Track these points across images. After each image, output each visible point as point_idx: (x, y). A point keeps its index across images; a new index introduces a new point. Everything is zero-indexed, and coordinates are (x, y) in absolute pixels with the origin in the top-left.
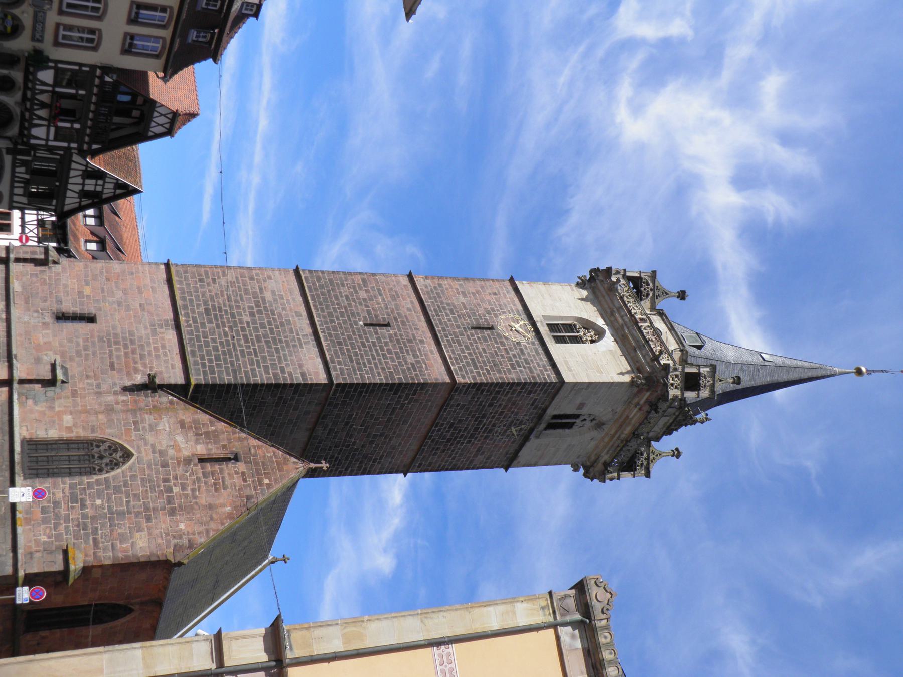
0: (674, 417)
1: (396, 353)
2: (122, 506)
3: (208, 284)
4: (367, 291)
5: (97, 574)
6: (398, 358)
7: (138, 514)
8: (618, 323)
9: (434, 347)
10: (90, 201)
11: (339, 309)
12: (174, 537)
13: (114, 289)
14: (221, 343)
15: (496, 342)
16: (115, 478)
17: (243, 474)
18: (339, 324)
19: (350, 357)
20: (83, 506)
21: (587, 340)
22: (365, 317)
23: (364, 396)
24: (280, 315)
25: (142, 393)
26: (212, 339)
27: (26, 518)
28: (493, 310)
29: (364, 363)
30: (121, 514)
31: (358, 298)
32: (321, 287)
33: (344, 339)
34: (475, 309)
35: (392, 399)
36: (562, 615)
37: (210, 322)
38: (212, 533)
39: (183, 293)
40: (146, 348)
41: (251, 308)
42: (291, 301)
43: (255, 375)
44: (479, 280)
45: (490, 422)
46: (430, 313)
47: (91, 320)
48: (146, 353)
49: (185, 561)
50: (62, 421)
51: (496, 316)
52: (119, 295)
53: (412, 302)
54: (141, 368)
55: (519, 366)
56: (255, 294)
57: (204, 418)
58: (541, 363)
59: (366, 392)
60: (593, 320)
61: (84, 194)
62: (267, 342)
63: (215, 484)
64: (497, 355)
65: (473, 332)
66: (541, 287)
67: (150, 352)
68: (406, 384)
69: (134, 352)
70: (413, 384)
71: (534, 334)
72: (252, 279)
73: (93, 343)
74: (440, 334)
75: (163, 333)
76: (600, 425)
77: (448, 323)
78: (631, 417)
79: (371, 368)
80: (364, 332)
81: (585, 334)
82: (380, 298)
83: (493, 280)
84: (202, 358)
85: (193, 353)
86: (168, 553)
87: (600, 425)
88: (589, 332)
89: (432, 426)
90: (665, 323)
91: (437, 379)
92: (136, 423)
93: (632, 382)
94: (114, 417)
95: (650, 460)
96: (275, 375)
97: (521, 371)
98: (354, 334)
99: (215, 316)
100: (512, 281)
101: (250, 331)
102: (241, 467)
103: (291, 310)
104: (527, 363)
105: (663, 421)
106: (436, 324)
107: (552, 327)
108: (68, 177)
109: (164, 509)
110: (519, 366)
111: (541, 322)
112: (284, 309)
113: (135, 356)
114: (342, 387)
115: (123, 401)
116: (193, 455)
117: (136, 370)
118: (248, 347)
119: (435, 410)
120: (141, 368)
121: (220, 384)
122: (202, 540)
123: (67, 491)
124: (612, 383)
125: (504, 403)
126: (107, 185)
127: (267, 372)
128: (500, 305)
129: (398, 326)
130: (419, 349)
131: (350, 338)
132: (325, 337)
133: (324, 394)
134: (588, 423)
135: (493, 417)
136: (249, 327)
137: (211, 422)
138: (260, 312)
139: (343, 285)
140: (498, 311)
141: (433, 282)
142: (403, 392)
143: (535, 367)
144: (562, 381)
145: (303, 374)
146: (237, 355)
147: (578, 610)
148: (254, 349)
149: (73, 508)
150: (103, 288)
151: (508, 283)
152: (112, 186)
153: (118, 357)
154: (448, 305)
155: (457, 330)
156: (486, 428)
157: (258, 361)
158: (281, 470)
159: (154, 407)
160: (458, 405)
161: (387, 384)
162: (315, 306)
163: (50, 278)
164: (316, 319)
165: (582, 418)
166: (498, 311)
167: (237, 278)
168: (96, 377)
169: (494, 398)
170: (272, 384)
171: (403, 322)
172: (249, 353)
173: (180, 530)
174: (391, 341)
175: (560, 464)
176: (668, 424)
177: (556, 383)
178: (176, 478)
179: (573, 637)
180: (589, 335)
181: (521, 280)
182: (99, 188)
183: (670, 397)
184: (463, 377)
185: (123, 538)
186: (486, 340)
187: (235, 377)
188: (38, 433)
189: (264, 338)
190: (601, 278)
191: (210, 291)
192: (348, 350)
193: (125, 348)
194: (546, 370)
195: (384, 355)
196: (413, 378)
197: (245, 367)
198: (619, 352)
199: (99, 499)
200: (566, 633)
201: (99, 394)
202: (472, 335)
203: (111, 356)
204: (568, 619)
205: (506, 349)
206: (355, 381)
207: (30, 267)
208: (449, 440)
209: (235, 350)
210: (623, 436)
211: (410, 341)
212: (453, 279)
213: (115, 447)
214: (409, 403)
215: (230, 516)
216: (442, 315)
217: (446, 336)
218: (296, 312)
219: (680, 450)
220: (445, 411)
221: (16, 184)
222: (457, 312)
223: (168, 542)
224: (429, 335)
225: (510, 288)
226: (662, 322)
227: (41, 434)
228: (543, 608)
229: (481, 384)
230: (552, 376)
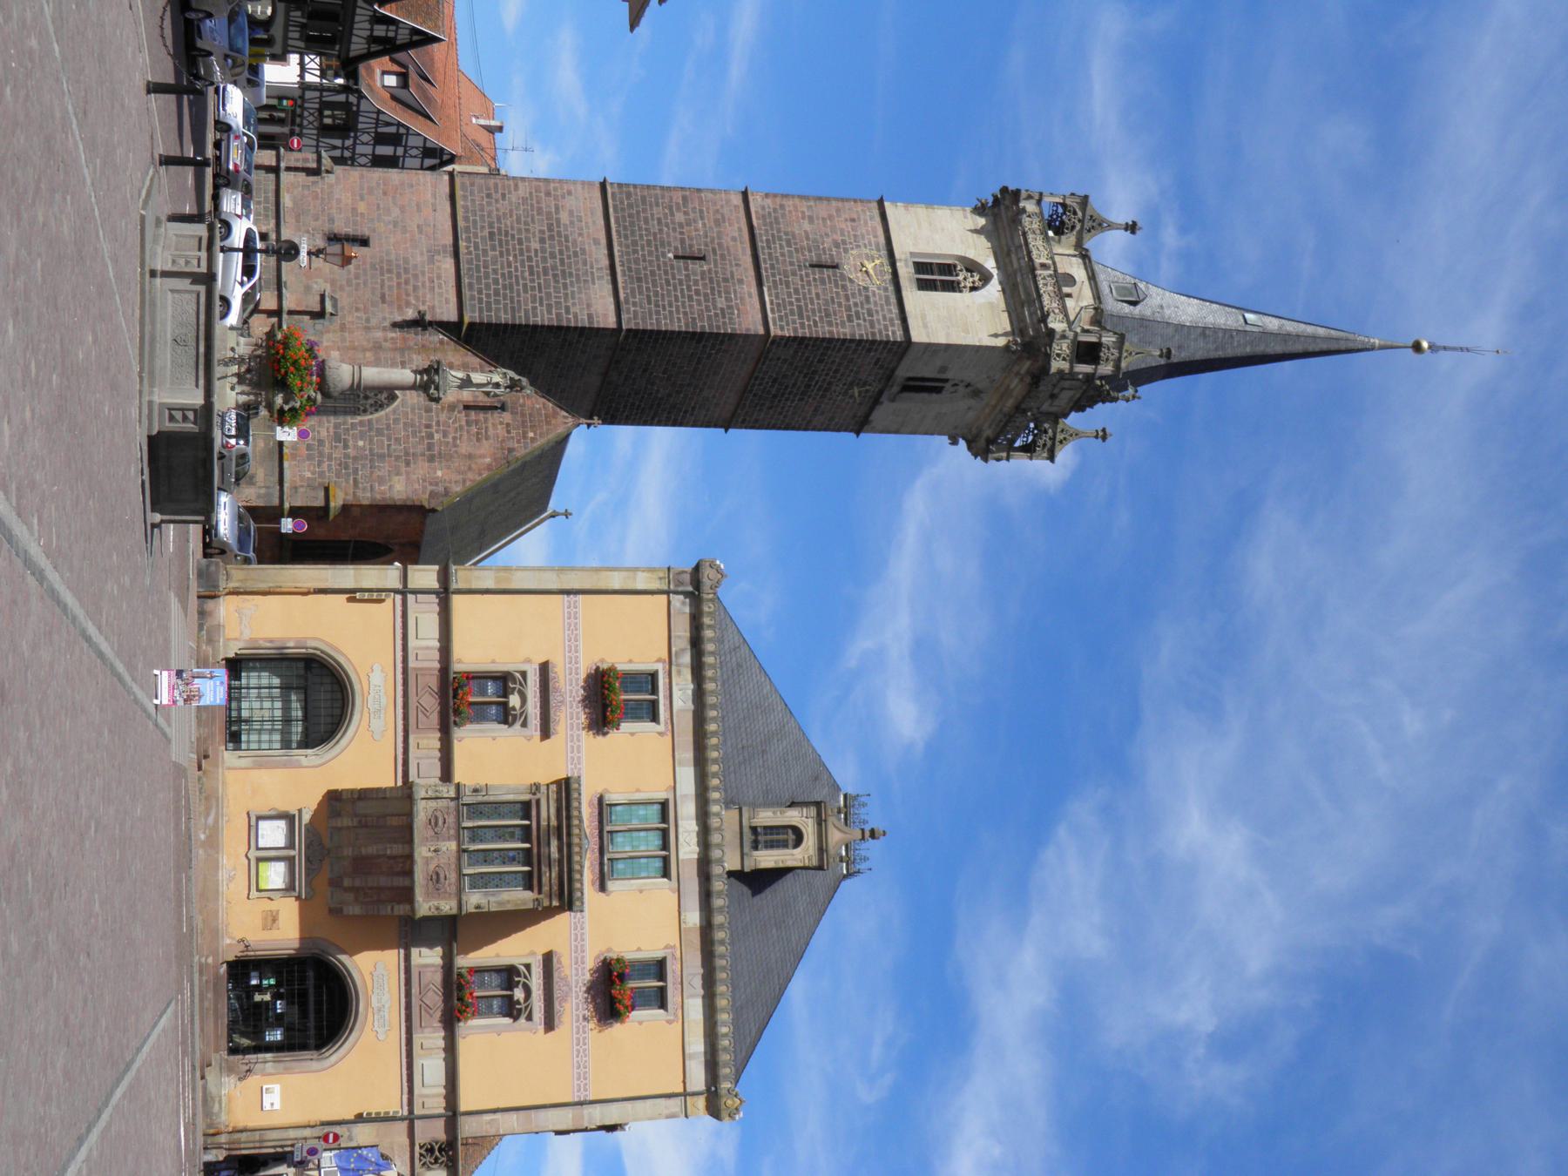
1: (706, 295)
2: (383, 448)
3: (497, 201)
4: (686, 213)
5: (356, 512)
7: (398, 458)
8: (1012, 266)
9: (754, 290)
10: (381, 48)
11: (646, 235)
12: (431, 484)
14: (503, 275)
15: (837, 286)
16: (378, 420)
17: (508, 425)
18: (643, 255)
19: (648, 297)
20: (346, 446)
21: (965, 287)
22: (676, 248)
24: (575, 241)
25: (412, 330)
26: (493, 270)
27: (292, 454)
28: (844, 242)
29: (664, 306)
30: (381, 457)
31: (673, 223)
33: (646, 275)
34: (820, 240)
36: (676, 586)
37: (493, 249)
38: (468, 484)
39: (467, 211)
40: (421, 278)
41: (542, 232)
42: (590, 224)
43: (535, 315)
44: (837, 199)
45: (824, 380)
48: (420, 284)
49: (439, 508)
51: (846, 251)
52: (396, 212)
53: (740, 229)
54: (413, 302)
55: (858, 318)
56: (549, 213)
58: (888, 316)
59: (663, 339)
60: (980, 260)
61: (372, 39)
62: (555, 276)
63: (478, 433)
64: (833, 302)
66: (921, 211)
68: (711, 334)
69: (407, 282)
71: (890, 277)
72: (548, 194)
75: (439, 261)
76: (977, 393)
77: (780, 258)
78: (1012, 386)
79: (671, 312)
80: (672, 268)
81: (965, 279)
83: (855, 201)
84: (480, 292)
85: (471, 285)
86: (424, 499)
87: (977, 393)
88: (972, 276)
89: (750, 379)
90: (1086, 269)
91: (748, 329)
93: (1007, 348)
94: (382, 355)
95: (1057, 440)
97: (859, 325)
98: (659, 269)
99: (500, 241)
100: (881, 203)
101: (537, 261)
102: (507, 417)
103: (589, 236)
104: (870, 313)
106: (765, 259)
107: (921, 267)
108: (353, 22)
109: (423, 455)
110: (858, 318)
111: (906, 260)
112: (580, 235)
113: (408, 287)
114: (634, 333)
115: (392, 338)
116: (459, 401)
117: (408, 304)
118: (532, 281)
120: (413, 302)
122: (458, 489)
123: (331, 430)
124: (980, 347)
126: (400, 31)
127: (549, 312)
128: (855, 236)
129: (715, 261)
130: (735, 291)
131: (653, 273)
132: (623, 271)
134: (961, 389)
135: (827, 375)
136: (536, 256)
137: (481, 366)
138: (552, 238)
139: (657, 205)
140: (851, 243)
143: (878, 320)
145: (590, 316)
146: (518, 290)
147: (691, 584)
148: (539, 284)
149: (336, 447)
150: (378, 205)
151: (874, 205)
152: (407, 32)
153: (390, 287)
154: (786, 234)
155: (789, 268)
157: (541, 298)
158: (548, 423)
159: (423, 346)
161: (686, 332)
162: (618, 232)
163: (322, 190)
164: (616, 248)
165: (951, 383)
166: (851, 243)
167: (531, 193)
168: (366, 310)
170: (553, 326)
171: (723, 257)
172: (533, 288)
173: (438, 477)
174: (702, 279)
175: (932, 434)
176: (1075, 399)
177: (901, 342)
178: (438, 423)
179: (684, 603)
180: (971, 280)
181: (894, 201)
182: (391, 34)
183: (1053, 370)
184: (782, 328)
185: (381, 481)
186: (823, 282)
187: (513, 317)
189: (552, 270)
190: (1007, 202)
191: (497, 210)
192: (648, 289)
194: (893, 325)
195: (690, 298)
196: (718, 327)
197: (526, 305)
198: (1003, 305)
199: (361, 439)
200: (677, 600)
201: (368, 329)
203: (382, 286)
204: (680, 589)
206: (649, 328)
207: (301, 176)
208: (775, 396)
209: (518, 284)
210: (1006, 410)
211: (726, 280)
212: (802, 197)
215: (489, 467)
217: (773, 275)
218: (594, 240)
219: (1108, 431)
221: (291, 28)
222: (796, 244)
223: (424, 487)
224: (751, 273)
225: (876, 212)
226: (1082, 266)
228: (660, 578)
229: (803, 338)
230: (898, 333)
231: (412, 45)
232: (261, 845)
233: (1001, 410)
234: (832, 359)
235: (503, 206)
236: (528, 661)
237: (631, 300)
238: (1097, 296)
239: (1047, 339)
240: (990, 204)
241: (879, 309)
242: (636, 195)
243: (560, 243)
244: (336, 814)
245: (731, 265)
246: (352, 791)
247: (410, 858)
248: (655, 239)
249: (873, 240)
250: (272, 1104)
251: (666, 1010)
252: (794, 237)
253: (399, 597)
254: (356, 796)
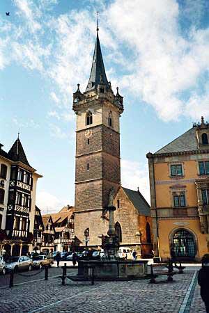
61: (51, 230)
231: (52, 222)
238: (92, 90)
253: (159, 219)
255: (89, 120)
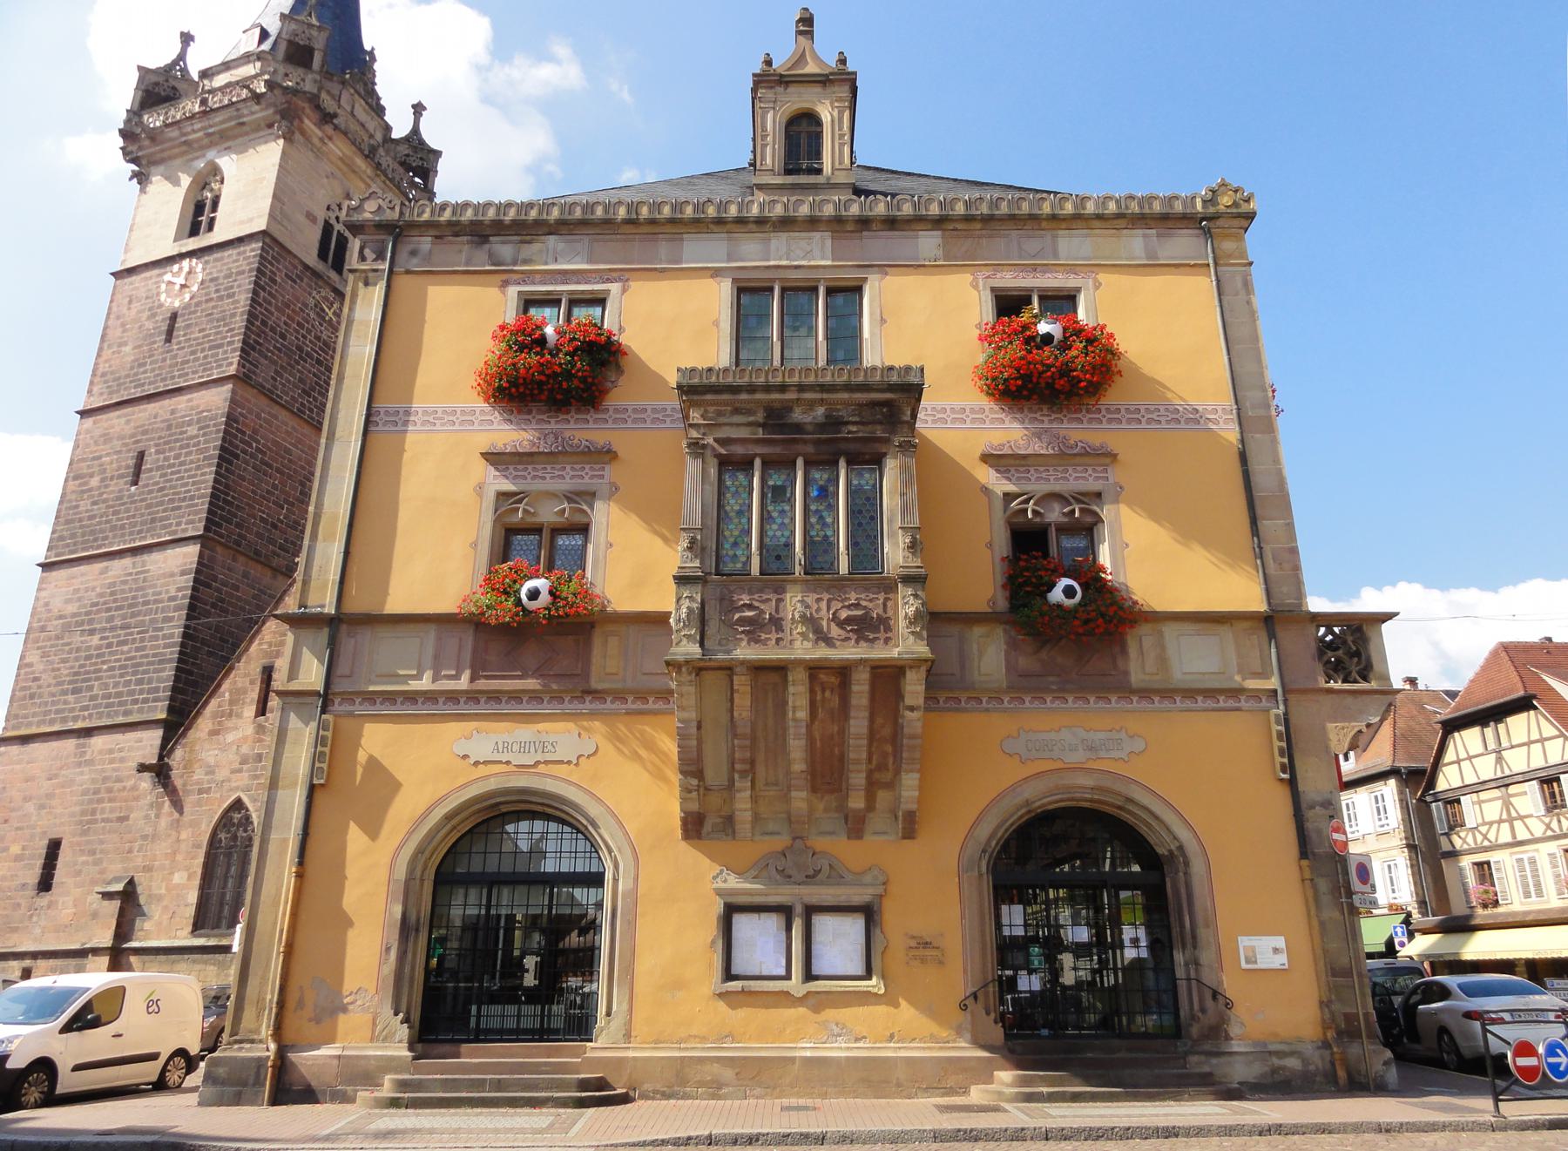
0: (356, 96)
1: (181, 447)
3: (39, 687)
4: (91, 476)
6: (188, 446)
13: (19, 813)
14: (122, 676)
22: (126, 483)
23: (233, 497)
24: (101, 595)
28: (150, 309)
29: (185, 492)
31: (100, 487)
32: (73, 536)
33: (149, 514)
35: (247, 463)
37: (91, 688)
39: (43, 722)
43: (172, 636)
46: (138, 395)
47: (54, 847)
50: (179, 884)
51: (161, 306)
52: (30, 807)
53: (119, 417)
54: (133, 782)
55: (232, 287)
57: (213, 704)
58: (235, 258)
59: (228, 494)
62: (133, 615)
65: (174, 341)
67: (114, 770)
69: (110, 790)
70: (226, 431)
73: (88, 842)
74: (168, 385)
79: (194, 483)
82: (104, 459)
84: (135, 702)
85: (126, 713)
91: (225, 400)
92: (200, 792)
96: (177, 609)
97: (239, 286)
101: (113, 637)
104: (227, 277)
105: (361, 111)
106: (155, 389)
110: (232, 287)
113: (115, 789)
114: (210, 523)
117: (135, 788)
118: (134, 641)
119: (276, 409)
121: (174, 681)
125: (283, 319)
127: (171, 619)
128: (147, 298)
131: (149, 506)
133: (219, 549)
136: (107, 638)
138: (91, 622)
139: (77, 507)
141: (98, 383)
142: (237, 447)
143: (238, 267)
144: (264, 233)
145: (183, 573)
146: (142, 657)
148: (139, 633)
154: (132, 368)
155: (168, 362)
156: (320, 348)
160: (273, 378)
161: (219, 466)
162: (99, 547)
165: (333, 221)
167: (38, 648)
169: (273, 330)
171: (145, 432)
172: (142, 640)
174: (164, 452)
176: (367, 107)
184: (231, 364)
186: (188, 326)
187: (170, 661)
188: (188, 915)
191: (49, 686)
193: (103, 802)
194: (245, 252)
195: (181, 464)
197: (158, 647)
202: (179, 343)
205: (207, 301)
209: (134, 658)
210: (369, 171)
211: (169, 427)
213: (225, 821)
214: (258, 442)
216: (145, 378)
217: (173, 377)
218: (101, 574)
220: (281, 398)
227: (190, 912)
229: (244, 342)
232: (782, 972)
233: (369, 177)
234: (282, 324)
235: (47, 678)
236: (480, 488)
237: (173, 528)
239: (276, 92)
240: (136, 168)
241: (225, 267)
242: (63, 530)
243: (98, 612)
244: (728, 824)
245: (155, 423)
246: (686, 790)
247: (815, 669)
248: (112, 506)
249: (153, 280)
250: (1276, 950)
251: (1078, 290)
252: (136, 360)
254: (695, 782)
255: (199, 215)
